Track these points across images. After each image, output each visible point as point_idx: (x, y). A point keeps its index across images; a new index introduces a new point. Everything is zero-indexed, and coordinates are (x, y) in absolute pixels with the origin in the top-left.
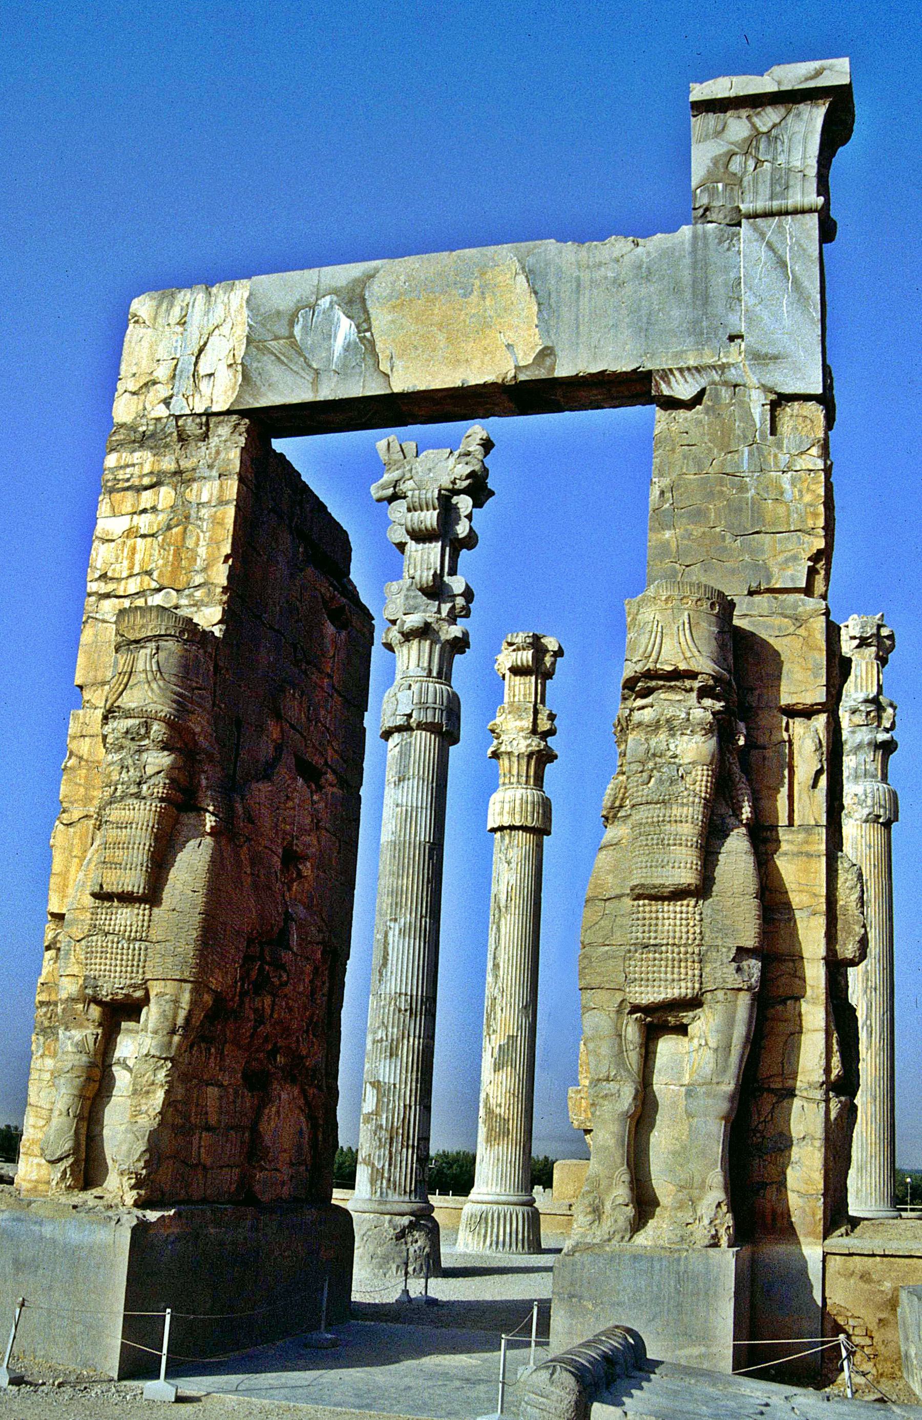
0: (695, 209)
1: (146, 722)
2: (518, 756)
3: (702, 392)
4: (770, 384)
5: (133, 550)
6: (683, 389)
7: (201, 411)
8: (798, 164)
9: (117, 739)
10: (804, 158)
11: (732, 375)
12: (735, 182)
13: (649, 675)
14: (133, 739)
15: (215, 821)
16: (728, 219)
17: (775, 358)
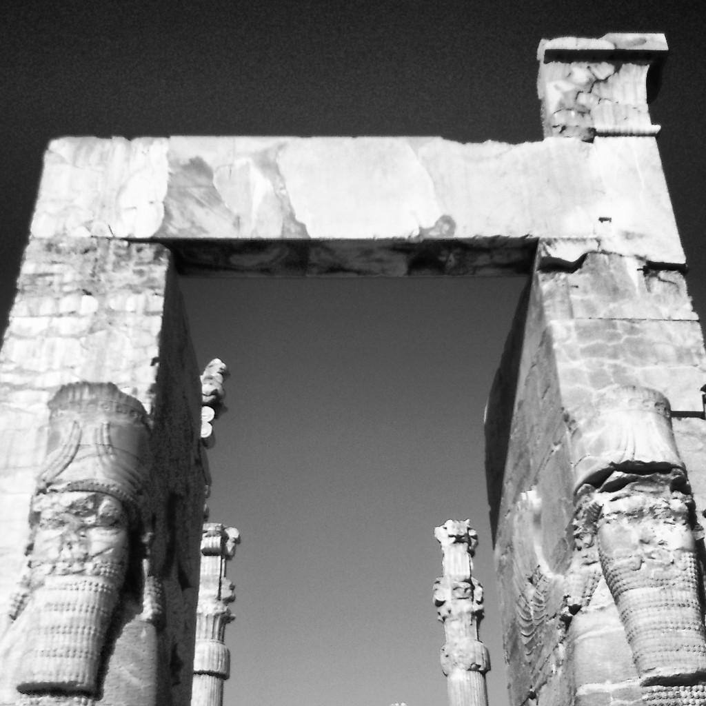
0: (555, 127)
1: (94, 496)
2: (207, 617)
3: (584, 258)
4: (642, 254)
5: (52, 349)
6: (569, 254)
7: (125, 235)
8: (633, 104)
9: (57, 514)
10: (636, 99)
11: (606, 246)
12: (584, 112)
13: (627, 467)
14: (77, 514)
15: (158, 608)
16: (583, 136)
17: (641, 236)
